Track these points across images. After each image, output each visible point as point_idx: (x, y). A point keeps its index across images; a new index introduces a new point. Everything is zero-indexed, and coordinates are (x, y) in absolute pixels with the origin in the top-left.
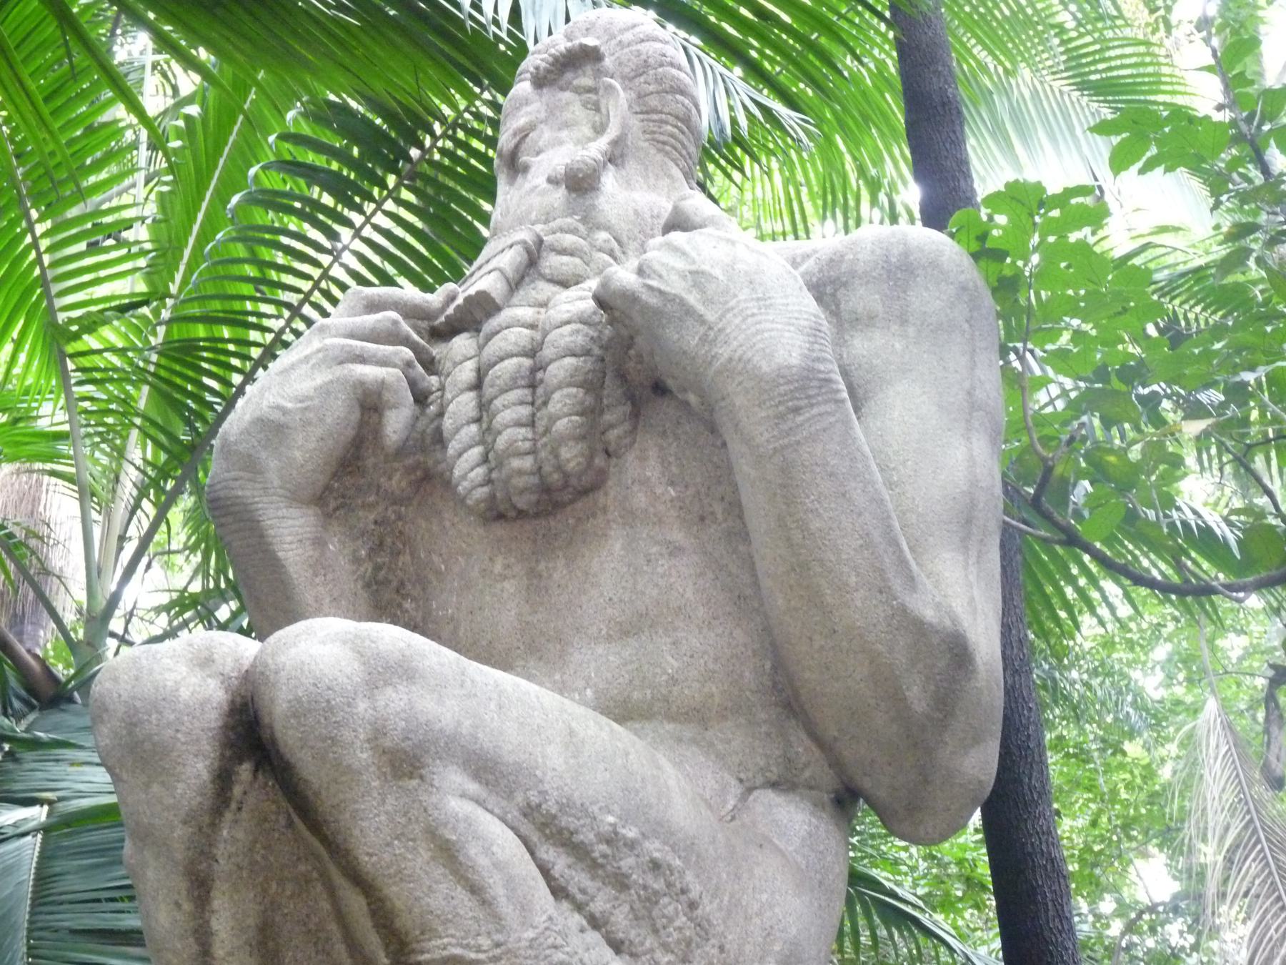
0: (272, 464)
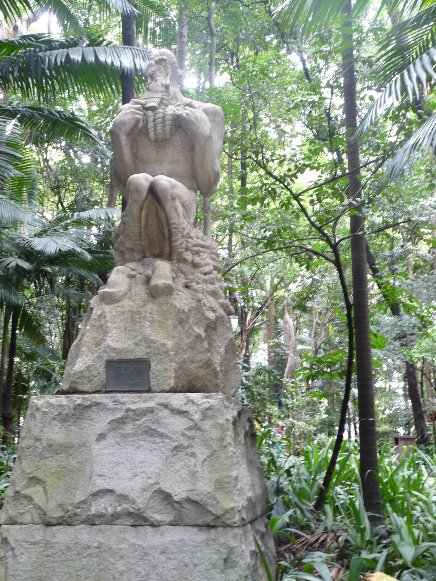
0: (123, 129)
